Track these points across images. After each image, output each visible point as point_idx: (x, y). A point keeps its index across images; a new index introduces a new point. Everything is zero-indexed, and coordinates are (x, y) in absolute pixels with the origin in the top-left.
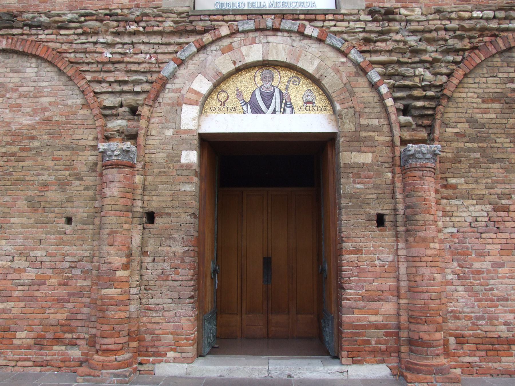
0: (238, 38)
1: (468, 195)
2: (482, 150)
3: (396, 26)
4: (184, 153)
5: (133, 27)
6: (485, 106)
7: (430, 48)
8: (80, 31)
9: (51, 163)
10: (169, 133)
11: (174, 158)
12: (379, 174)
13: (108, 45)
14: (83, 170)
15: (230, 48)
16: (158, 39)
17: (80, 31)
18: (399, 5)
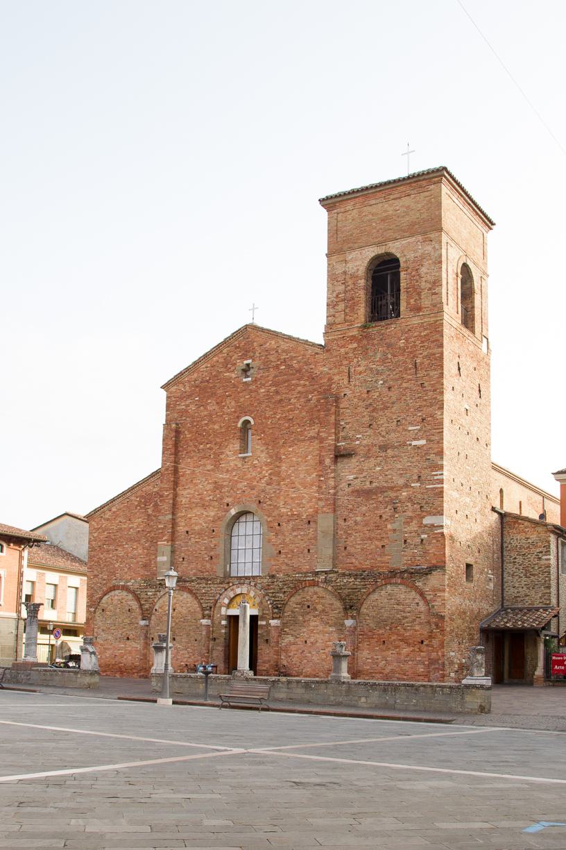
5: (209, 582)
15: (232, 590)
16: (216, 586)
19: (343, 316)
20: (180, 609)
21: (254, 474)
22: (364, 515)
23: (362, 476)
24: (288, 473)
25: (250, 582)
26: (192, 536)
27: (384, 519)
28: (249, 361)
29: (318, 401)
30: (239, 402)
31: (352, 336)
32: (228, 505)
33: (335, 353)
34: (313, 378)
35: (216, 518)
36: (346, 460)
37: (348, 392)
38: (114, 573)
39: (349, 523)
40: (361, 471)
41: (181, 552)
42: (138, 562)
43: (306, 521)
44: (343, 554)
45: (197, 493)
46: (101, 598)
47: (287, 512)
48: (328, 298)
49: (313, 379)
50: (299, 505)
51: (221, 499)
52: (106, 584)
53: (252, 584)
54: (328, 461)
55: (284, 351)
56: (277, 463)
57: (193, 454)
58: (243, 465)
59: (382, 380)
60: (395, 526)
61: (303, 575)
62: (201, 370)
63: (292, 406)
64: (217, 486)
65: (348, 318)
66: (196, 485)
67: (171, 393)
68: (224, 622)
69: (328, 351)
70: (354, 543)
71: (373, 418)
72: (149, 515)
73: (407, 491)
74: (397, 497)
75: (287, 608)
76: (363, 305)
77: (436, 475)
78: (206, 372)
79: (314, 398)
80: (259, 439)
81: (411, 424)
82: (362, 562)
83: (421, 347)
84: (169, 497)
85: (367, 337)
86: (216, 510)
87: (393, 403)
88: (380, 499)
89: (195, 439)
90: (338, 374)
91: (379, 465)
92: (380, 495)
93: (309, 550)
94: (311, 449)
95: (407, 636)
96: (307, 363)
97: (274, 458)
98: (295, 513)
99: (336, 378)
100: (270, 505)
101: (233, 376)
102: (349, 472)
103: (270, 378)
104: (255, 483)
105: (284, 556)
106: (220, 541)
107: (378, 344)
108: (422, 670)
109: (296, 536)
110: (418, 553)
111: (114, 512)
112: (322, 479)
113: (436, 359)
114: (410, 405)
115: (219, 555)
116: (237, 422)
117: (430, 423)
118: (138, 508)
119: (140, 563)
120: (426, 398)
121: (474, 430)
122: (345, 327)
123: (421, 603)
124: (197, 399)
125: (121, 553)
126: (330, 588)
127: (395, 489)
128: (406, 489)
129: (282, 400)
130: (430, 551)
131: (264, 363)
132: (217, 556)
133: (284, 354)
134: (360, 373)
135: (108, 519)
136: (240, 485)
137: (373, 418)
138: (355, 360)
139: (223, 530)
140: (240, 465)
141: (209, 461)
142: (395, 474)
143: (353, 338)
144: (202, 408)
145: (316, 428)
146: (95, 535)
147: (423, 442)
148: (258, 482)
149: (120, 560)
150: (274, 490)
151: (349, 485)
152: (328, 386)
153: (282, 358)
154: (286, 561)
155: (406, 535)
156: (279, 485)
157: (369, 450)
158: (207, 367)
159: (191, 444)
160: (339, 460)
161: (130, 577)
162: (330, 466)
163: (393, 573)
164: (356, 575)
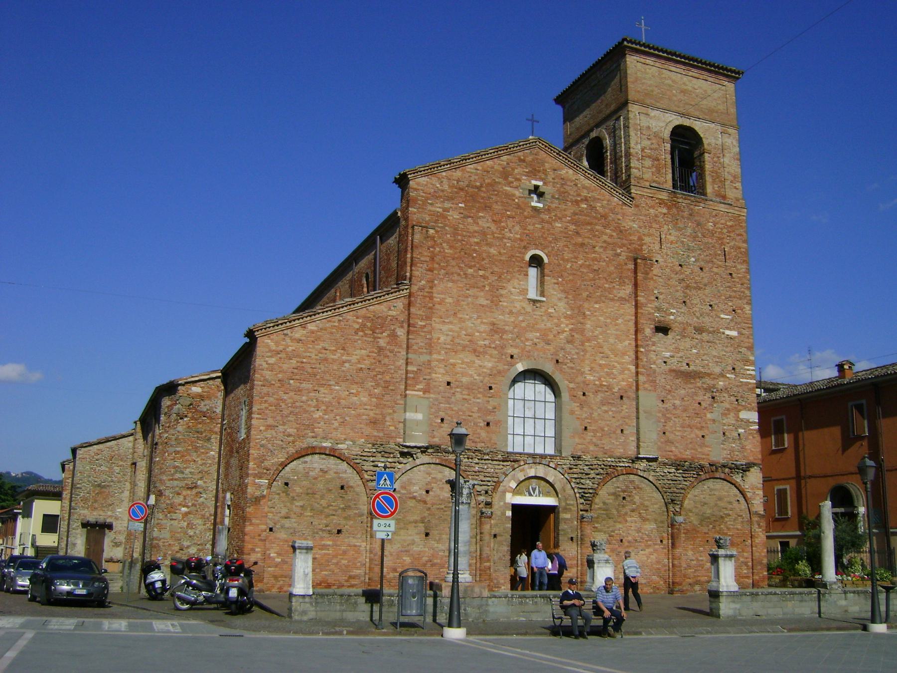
0: (526, 466)
1: (600, 531)
2: (607, 514)
3: (580, 462)
4: (507, 512)
5: (487, 457)
6: (609, 497)
7: (592, 472)
8: (466, 456)
10: (502, 503)
11: (504, 514)
12: (572, 522)
16: (495, 462)
17: (466, 456)
18: (583, 454)
19: (650, 174)
20: (438, 492)
21: (549, 325)
22: (683, 399)
23: (679, 355)
24: (595, 334)
26: (458, 390)
27: (703, 407)
30: (525, 229)
31: (661, 199)
32: (512, 357)
34: (620, 231)
35: (495, 372)
37: (660, 260)
38: (311, 427)
39: (668, 405)
40: (677, 350)
41: (439, 410)
42: (359, 415)
43: (618, 395)
44: (662, 440)
45: (464, 332)
46: (284, 465)
49: (621, 231)
50: (608, 374)
52: (294, 442)
54: (648, 331)
55: (584, 187)
56: (580, 318)
57: (456, 277)
58: (533, 310)
59: (693, 257)
62: (469, 170)
64: (495, 329)
66: (462, 320)
67: (418, 184)
68: (509, 513)
69: (637, 206)
70: (674, 429)
72: (380, 349)
73: (723, 381)
74: (714, 385)
75: (597, 500)
77: (748, 370)
78: (477, 175)
80: (555, 283)
81: (723, 311)
82: (682, 451)
84: (425, 330)
85: (676, 205)
86: (496, 360)
87: (705, 285)
88: (699, 384)
91: (696, 347)
92: (698, 380)
93: (622, 431)
94: (621, 311)
96: (612, 211)
97: (576, 311)
98: (604, 383)
99: (647, 240)
100: (572, 368)
103: (568, 213)
104: (551, 337)
105: (592, 434)
108: (745, 571)
109: (606, 412)
110: (737, 448)
111: (312, 332)
113: (741, 253)
115: (499, 421)
116: (524, 254)
118: (361, 333)
119: (364, 417)
120: (735, 289)
124: (460, 205)
125: (325, 395)
126: (651, 478)
127: (711, 376)
129: (584, 244)
130: (747, 447)
131: (560, 193)
132: (498, 423)
133: (585, 191)
136: (530, 335)
138: (666, 227)
141: (482, 294)
142: (711, 361)
143: (662, 202)
144: (470, 220)
146: (272, 361)
147: (734, 333)
148: (555, 336)
149: (324, 408)
152: (639, 245)
154: (594, 440)
155: (725, 427)
156: (583, 345)
157: (684, 329)
161: (344, 436)
162: (651, 338)
164: (679, 465)
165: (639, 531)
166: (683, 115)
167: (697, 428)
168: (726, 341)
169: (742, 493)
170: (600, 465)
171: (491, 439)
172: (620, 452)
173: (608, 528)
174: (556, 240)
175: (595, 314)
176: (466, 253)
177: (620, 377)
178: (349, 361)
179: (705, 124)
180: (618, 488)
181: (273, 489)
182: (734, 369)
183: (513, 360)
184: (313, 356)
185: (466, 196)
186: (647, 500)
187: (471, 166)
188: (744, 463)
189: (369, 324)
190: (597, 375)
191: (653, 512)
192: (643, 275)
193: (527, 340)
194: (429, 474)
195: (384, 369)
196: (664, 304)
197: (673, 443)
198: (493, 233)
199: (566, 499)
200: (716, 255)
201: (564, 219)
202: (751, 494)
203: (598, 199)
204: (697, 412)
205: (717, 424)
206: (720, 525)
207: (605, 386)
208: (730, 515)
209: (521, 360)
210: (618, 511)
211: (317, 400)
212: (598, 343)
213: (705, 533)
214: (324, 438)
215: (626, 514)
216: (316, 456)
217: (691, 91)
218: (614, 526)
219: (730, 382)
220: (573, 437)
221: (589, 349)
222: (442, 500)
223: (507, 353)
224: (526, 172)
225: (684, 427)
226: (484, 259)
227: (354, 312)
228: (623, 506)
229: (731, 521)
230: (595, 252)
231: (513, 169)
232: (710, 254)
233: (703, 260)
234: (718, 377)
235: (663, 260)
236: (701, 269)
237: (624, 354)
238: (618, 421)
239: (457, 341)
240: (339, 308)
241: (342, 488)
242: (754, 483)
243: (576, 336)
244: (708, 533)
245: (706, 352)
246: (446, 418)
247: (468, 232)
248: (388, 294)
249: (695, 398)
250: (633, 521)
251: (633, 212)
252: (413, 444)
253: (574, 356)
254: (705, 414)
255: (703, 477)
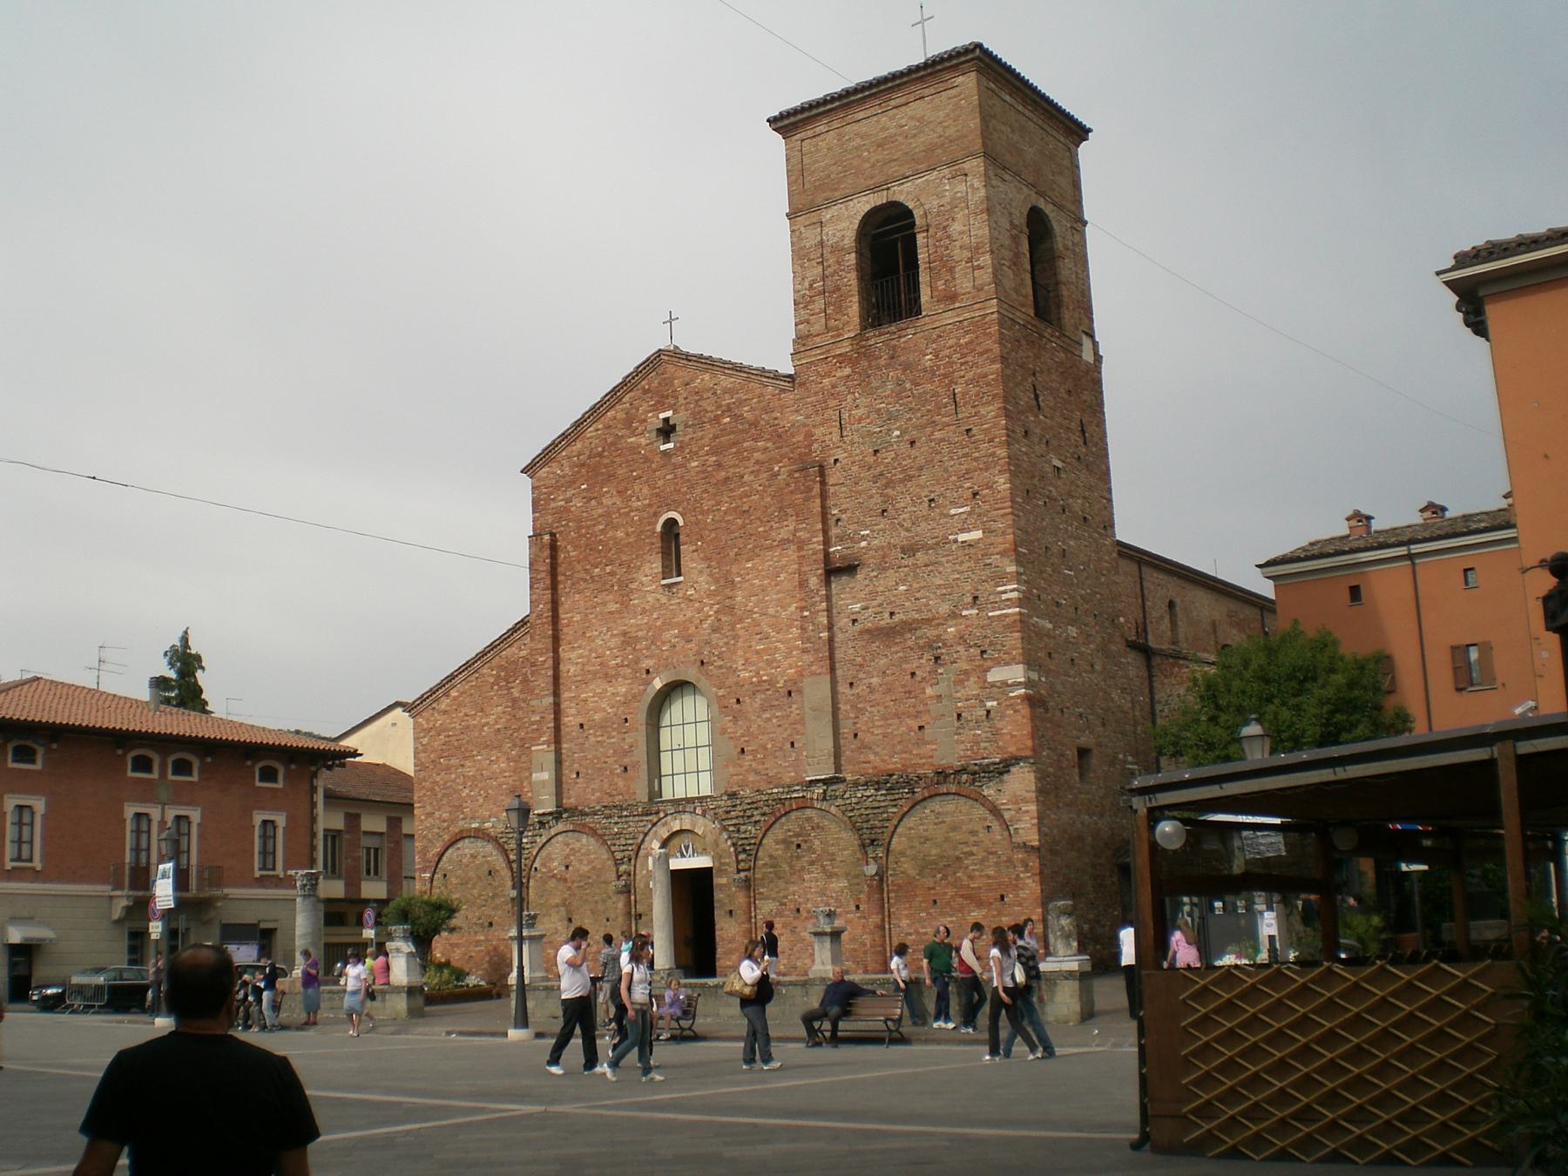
0: (669, 817)
1: (767, 898)
2: (775, 873)
9: (597, 891)
10: (644, 872)
12: (730, 889)
13: (617, 823)
14: (611, 894)
15: (666, 823)
16: (637, 818)
21: (689, 614)
22: (884, 672)
23: (875, 603)
24: (749, 608)
25: (695, 808)
26: (591, 731)
27: (918, 678)
28: (669, 414)
29: (790, 475)
30: (655, 488)
32: (648, 672)
33: (814, 388)
34: (778, 437)
36: (844, 578)
37: (841, 455)
38: (459, 808)
39: (860, 689)
40: (873, 594)
42: (500, 785)
44: (853, 746)
45: (594, 655)
47: (751, 678)
48: (796, 291)
49: (780, 436)
51: (636, 663)
52: (448, 828)
53: (699, 811)
54: (814, 581)
56: (728, 592)
57: (583, 585)
58: (669, 600)
59: (897, 429)
60: (941, 689)
61: (786, 790)
62: (588, 435)
63: (747, 488)
65: (832, 323)
67: (538, 480)
69: (802, 384)
70: (871, 725)
71: (887, 499)
72: (514, 700)
73: (955, 625)
74: (939, 636)
76: (856, 299)
77: (1005, 592)
79: (782, 469)
80: (694, 551)
81: (954, 504)
83: (962, 364)
84: (546, 666)
86: (629, 681)
88: (909, 643)
89: (586, 558)
90: (822, 424)
91: (904, 581)
93: (792, 744)
95: (973, 888)
98: (765, 678)
99: (818, 432)
100: (720, 667)
101: (643, 441)
102: (851, 598)
103: (706, 441)
105: (751, 757)
106: (639, 737)
107: (887, 366)
109: (769, 720)
110: (984, 735)
111: (455, 698)
112: (806, 613)
114: (950, 469)
117: (987, 499)
118: (496, 687)
120: (977, 454)
121: (1077, 505)
122: (828, 338)
123: (996, 826)
124: (583, 487)
126: (833, 809)
128: (954, 622)
133: (727, 396)
134: (860, 420)
135: (445, 712)
136: (667, 635)
137: (887, 499)
139: (642, 716)
140: (664, 600)
143: (843, 359)
144: (593, 502)
145: (791, 524)
146: (425, 741)
147: (977, 535)
149: (470, 783)
150: (726, 640)
151: (854, 621)
152: (805, 447)
153: (724, 403)
155: (959, 704)
156: (733, 630)
158: (598, 430)
159: (579, 567)
160: (832, 578)
162: (818, 590)
163: (942, 775)
164: (877, 783)
165: (822, 893)
166: (874, 189)
167: (909, 717)
168: (960, 553)
169: (995, 811)
170: (767, 801)
171: (629, 789)
172: (790, 777)
173: (778, 892)
174: (692, 487)
175: (747, 578)
176: (591, 550)
177: (785, 664)
178: (487, 723)
179: (920, 180)
180: (789, 830)
181: (435, 883)
182: (976, 598)
183: (650, 676)
184: (458, 727)
185: (588, 472)
186: (833, 845)
187: (591, 429)
188: (997, 760)
189: (503, 674)
190: (754, 668)
191: (842, 861)
192: (803, 495)
193: (664, 643)
194: (568, 844)
195: (519, 724)
196: (851, 527)
197: (870, 748)
198: (619, 509)
199: (721, 857)
200: (939, 408)
201: (701, 453)
202: (1013, 812)
203: (746, 400)
204: (907, 689)
205: (945, 702)
206: (955, 873)
207: (765, 681)
208: (973, 855)
209: (658, 674)
210: (791, 867)
211: (464, 776)
212: (754, 620)
213: (930, 889)
214: (472, 818)
215: (803, 869)
216: (467, 840)
217: (895, 135)
218: (786, 889)
219: (969, 622)
220: (727, 766)
221: (741, 632)
222: (580, 876)
223: (641, 669)
224: (652, 405)
225: (888, 719)
226: (611, 549)
227: (489, 664)
228: (798, 857)
229: (972, 864)
230: (743, 485)
231: (638, 409)
232: (929, 411)
233: (915, 427)
234: (946, 620)
235: (846, 455)
236: (912, 443)
237: (791, 626)
238: (786, 730)
239: (588, 668)
240: (473, 664)
241: (490, 873)
242: (1018, 793)
243: (724, 619)
244: (934, 888)
245: (922, 585)
246: (582, 771)
247: (591, 520)
248: (516, 631)
249: (904, 666)
250: (813, 878)
251: (797, 397)
252: (541, 811)
253: (724, 649)
254: (924, 689)
255: (918, 797)
